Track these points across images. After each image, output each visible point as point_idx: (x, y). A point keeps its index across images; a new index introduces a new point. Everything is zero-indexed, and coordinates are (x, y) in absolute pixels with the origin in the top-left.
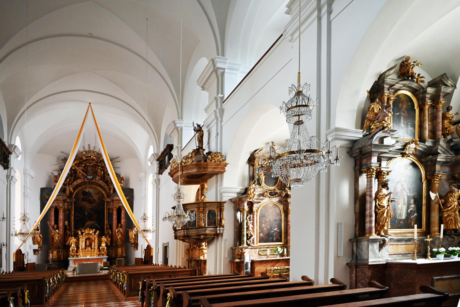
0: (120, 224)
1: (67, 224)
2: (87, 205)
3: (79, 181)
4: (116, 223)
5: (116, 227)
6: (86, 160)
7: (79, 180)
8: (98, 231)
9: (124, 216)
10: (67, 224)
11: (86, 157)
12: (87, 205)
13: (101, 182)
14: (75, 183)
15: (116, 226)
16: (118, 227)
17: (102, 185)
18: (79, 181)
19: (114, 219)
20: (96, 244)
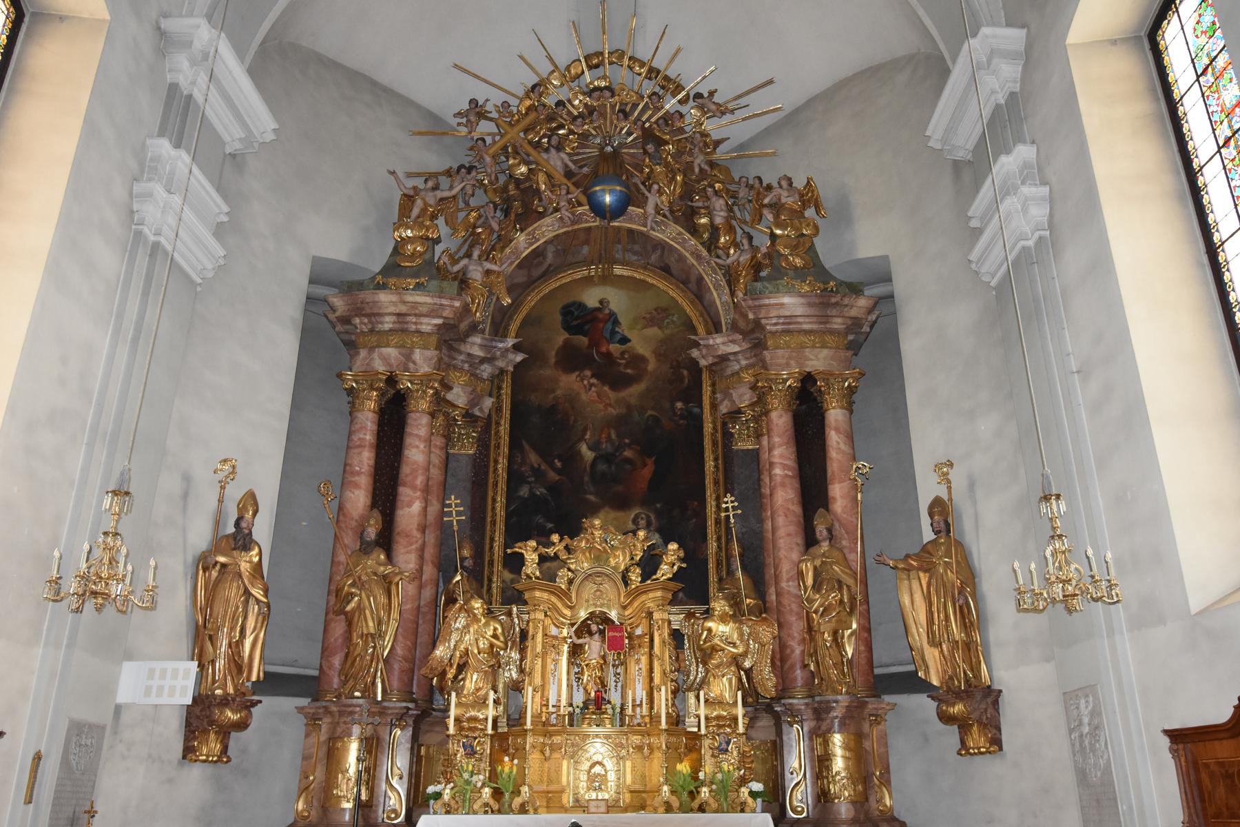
0: (821, 510)
1: (454, 519)
2: (593, 393)
3: (547, 228)
4: (797, 509)
6: (590, 110)
7: (548, 220)
8: (673, 546)
9: (842, 446)
10: (454, 519)
11: (590, 93)
12: (593, 393)
13: (669, 233)
14: (522, 242)
15: (792, 529)
16: (810, 541)
17: (681, 258)
18: (547, 228)
19: (778, 471)
20: (657, 680)
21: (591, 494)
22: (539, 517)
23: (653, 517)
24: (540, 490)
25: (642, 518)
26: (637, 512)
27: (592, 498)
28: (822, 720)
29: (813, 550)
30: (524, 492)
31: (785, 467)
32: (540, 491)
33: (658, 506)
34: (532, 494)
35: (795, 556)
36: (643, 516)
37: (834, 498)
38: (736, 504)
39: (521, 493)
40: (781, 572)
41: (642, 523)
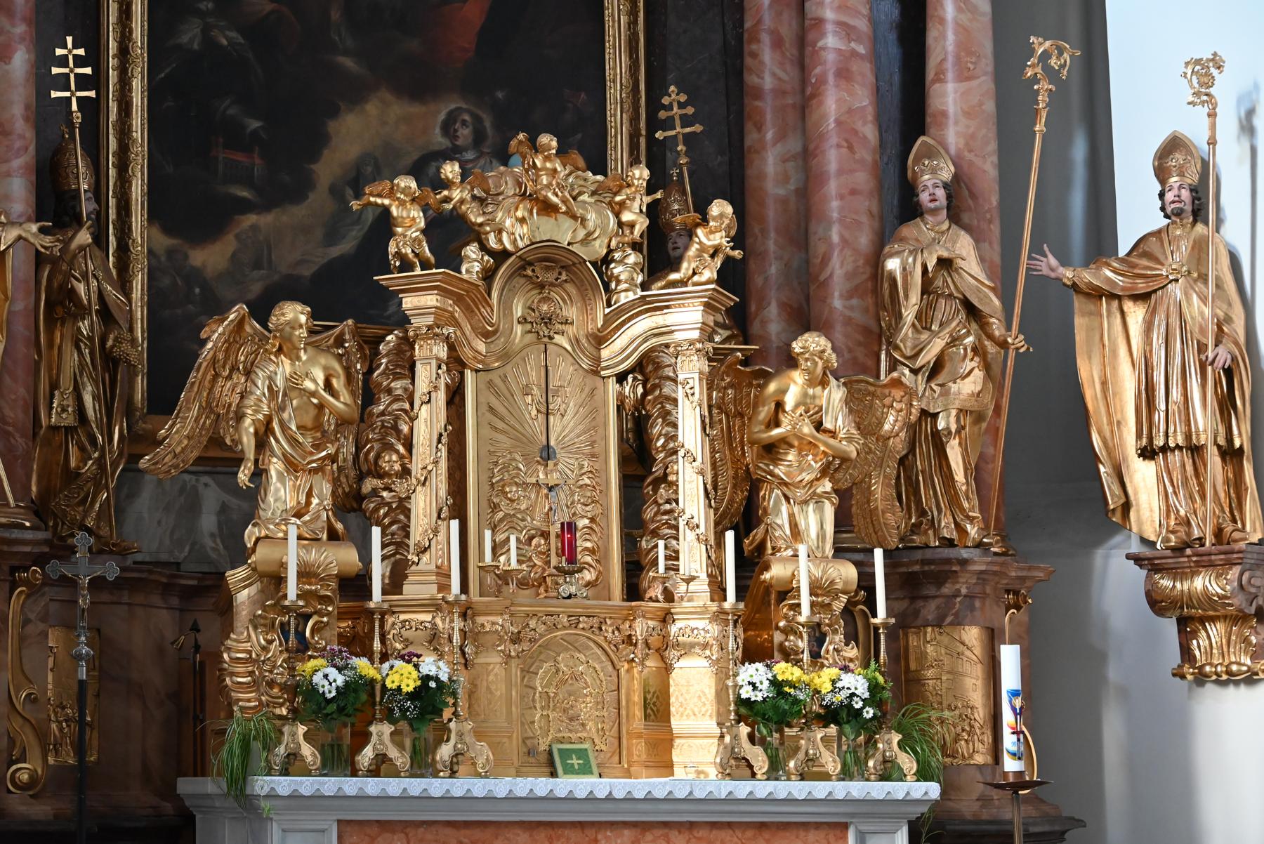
5: (865, 206)
15: (863, 179)
21: (346, 53)
22: (227, 102)
23: (488, 124)
24: (233, 34)
25: (464, 123)
26: (453, 106)
27: (348, 62)
28: (926, 598)
29: (908, 230)
30: (190, 35)
31: (846, 30)
32: (226, 38)
33: (500, 95)
34: (209, 42)
35: (864, 240)
36: (467, 117)
37: (944, 114)
38: (690, 110)
39: (185, 39)
40: (831, 275)
41: (465, 134)
